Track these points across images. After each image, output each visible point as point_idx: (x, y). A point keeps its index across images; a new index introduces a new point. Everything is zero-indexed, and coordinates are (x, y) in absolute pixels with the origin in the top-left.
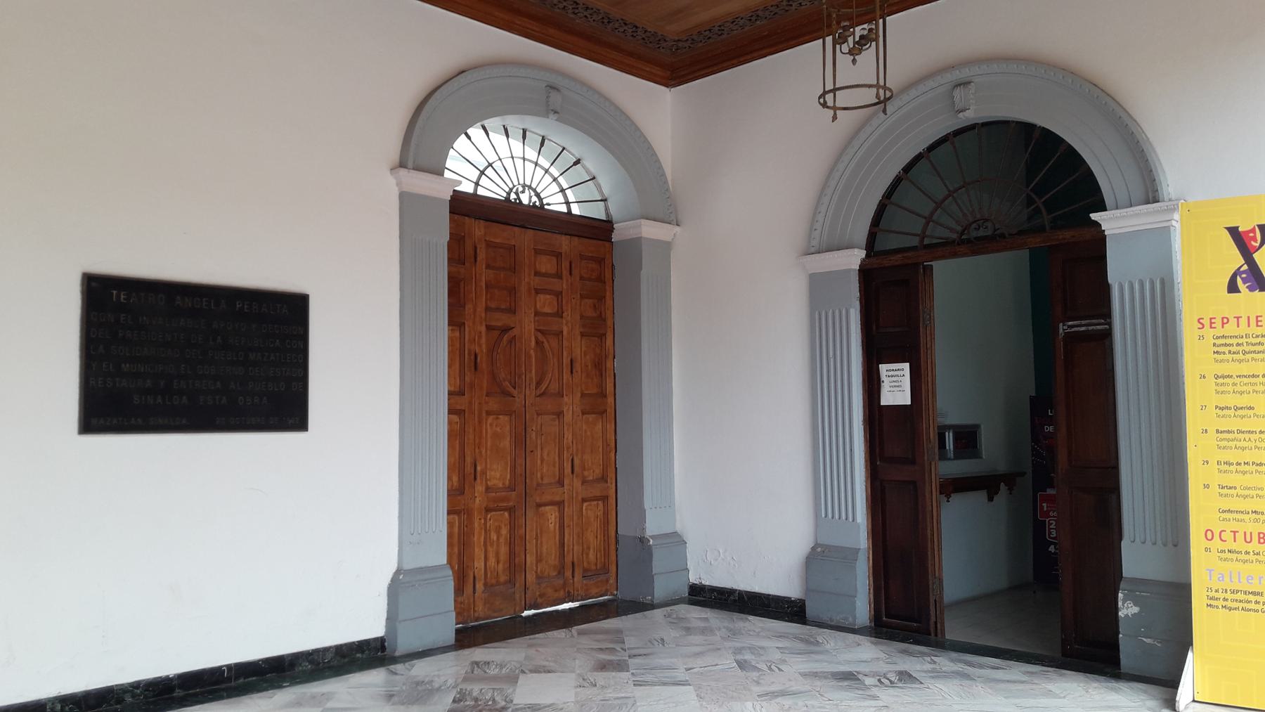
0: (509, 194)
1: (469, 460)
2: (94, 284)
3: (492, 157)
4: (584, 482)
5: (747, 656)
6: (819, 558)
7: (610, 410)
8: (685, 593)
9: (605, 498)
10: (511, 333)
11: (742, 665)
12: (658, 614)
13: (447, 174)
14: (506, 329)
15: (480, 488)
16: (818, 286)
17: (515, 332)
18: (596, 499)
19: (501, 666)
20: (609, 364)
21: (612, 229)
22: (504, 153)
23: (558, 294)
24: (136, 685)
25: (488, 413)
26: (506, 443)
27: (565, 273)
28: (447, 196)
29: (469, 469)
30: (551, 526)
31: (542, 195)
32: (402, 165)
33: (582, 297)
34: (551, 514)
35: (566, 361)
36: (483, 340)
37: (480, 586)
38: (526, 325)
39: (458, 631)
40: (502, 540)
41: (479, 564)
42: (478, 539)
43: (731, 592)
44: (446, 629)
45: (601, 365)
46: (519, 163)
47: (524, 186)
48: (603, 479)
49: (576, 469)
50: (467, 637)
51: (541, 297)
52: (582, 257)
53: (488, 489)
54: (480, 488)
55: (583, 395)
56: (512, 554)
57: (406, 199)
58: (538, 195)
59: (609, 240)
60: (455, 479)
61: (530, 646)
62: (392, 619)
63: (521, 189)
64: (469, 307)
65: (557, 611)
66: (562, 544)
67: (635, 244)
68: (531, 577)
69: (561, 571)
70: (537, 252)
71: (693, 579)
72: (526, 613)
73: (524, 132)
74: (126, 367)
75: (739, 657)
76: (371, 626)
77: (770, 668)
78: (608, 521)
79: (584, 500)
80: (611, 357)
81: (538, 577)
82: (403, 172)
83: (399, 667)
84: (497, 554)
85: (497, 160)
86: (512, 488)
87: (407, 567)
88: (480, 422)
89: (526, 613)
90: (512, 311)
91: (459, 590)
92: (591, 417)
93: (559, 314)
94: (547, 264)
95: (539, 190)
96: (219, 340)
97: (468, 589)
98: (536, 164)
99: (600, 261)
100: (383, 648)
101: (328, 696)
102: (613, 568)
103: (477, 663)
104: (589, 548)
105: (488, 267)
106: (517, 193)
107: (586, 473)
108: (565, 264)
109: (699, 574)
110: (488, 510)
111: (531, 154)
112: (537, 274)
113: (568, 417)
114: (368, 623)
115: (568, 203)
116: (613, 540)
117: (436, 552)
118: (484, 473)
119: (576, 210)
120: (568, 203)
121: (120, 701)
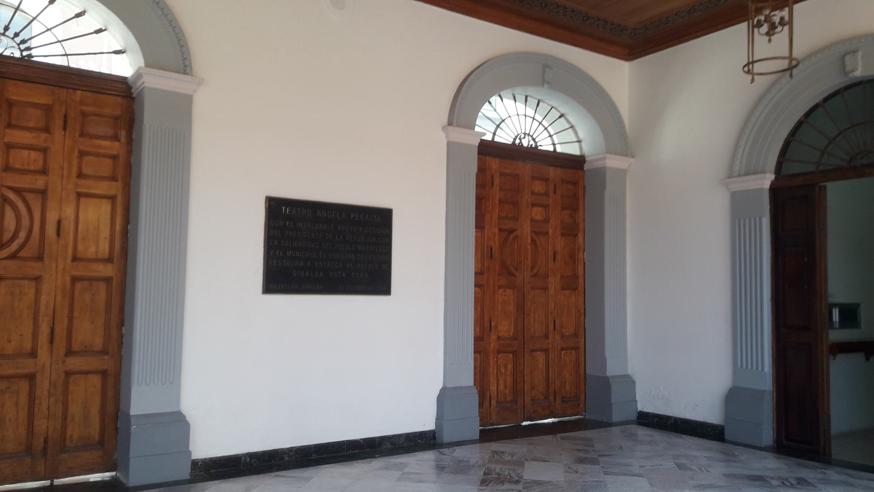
0: (515, 139)
1: (486, 318)
2: (272, 203)
4: (562, 336)
5: (683, 461)
6: (734, 397)
7: (581, 288)
8: (634, 417)
9: (577, 349)
10: (515, 233)
11: (680, 466)
12: (615, 430)
13: (477, 129)
14: (512, 231)
15: (494, 337)
16: (739, 204)
17: (518, 233)
18: (572, 349)
19: (512, 455)
20: (580, 255)
23: (546, 207)
25: (500, 287)
26: (511, 308)
27: (551, 191)
29: (487, 324)
30: (541, 366)
31: (537, 140)
32: (450, 123)
33: (562, 209)
34: (541, 358)
35: (551, 253)
36: (497, 238)
37: (494, 402)
38: (526, 229)
39: (481, 431)
40: (508, 372)
41: (493, 388)
42: (492, 370)
43: (668, 418)
44: (474, 429)
45: (573, 257)
46: (522, 118)
47: (525, 134)
48: (576, 335)
49: (557, 327)
50: (486, 436)
51: (535, 209)
52: (563, 181)
53: (499, 338)
54: (494, 337)
55: (562, 276)
56: (515, 383)
58: (534, 140)
59: (582, 168)
60: (478, 330)
61: (530, 444)
62: (439, 419)
63: (523, 136)
64: (488, 216)
65: (544, 424)
66: (548, 378)
67: (601, 173)
68: (528, 400)
69: (547, 397)
70: (533, 178)
71: (640, 407)
72: (525, 423)
73: (526, 97)
74: (289, 253)
75: (677, 461)
76: (426, 423)
77: (700, 469)
78: (580, 364)
79: (562, 349)
80: (582, 250)
81: (532, 400)
82: (450, 128)
83: (445, 450)
84: (505, 382)
85: (511, 119)
86: (514, 338)
87: (449, 386)
88: (494, 293)
89: (525, 423)
90: (516, 219)
91: (481, 405)
92: (567, 292)
93: (546, 221)
94: (539, 187)
95: (534, 137)
96: (341, 237)
97: (486, 404)
98: (534, 119)
99: (575, 183)
100: (434, 438)
101: (405, 465)
102: (583, 397)
103: (496, 452)
104: (565, 382)
105: (500, 189)
106: (520, 139)
107: (564, 331)
108: (551, 186)
109: (645, 404)
110: (499, 352)
111: (530, 112)
112: (533, 193)
113: (552, 291)
114: (423, 420)
115: (554, 144)
116: (582, 377)
117: (467, 379)
118: (496, 326)
119: (559, 149)
120: (554, 144)
121: (282, 459)
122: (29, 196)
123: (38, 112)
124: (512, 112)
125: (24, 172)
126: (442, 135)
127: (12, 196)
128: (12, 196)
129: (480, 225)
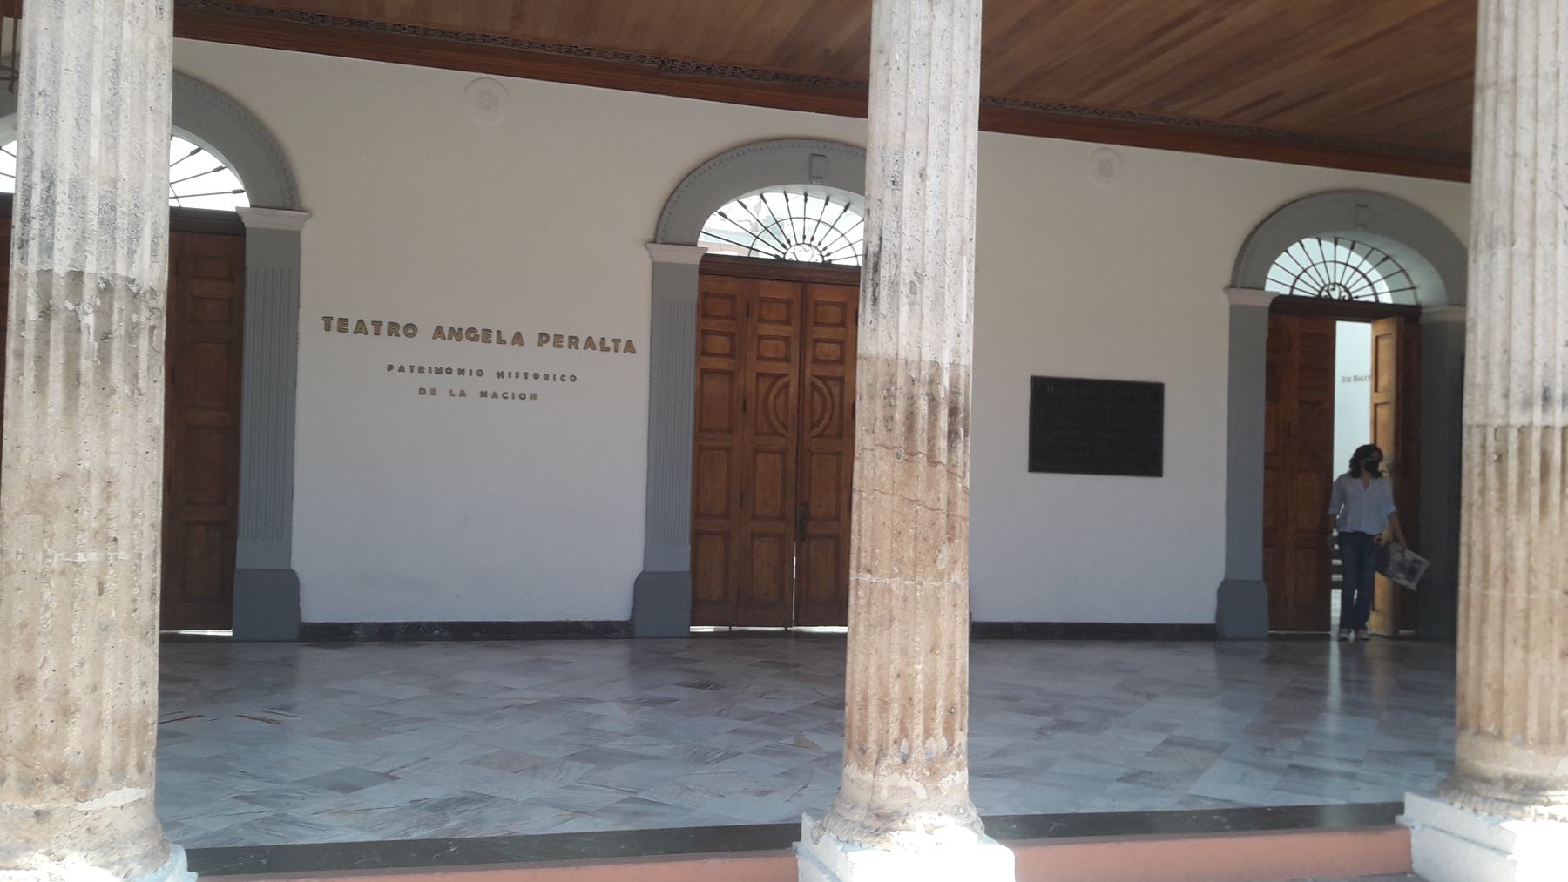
3: (1306, 264)
21: (1420, 313)
22: (1317, 258)
24: (1059, 624)
28: (1267, 303)
32: (1233, 286)
46: (1330, 266)
57: (1235, 310)
58: (1347, 290)
115: (1376, 294)
120: (1376, 294)
122: (830, 383)
123: (837, 310)
124: (1317, 258)
125: (826, 362)
126: (1225, 297)
127: (819, 383)
128: (819, 383)
129: (1272, 395)
